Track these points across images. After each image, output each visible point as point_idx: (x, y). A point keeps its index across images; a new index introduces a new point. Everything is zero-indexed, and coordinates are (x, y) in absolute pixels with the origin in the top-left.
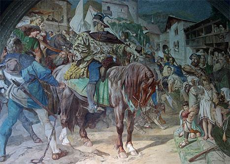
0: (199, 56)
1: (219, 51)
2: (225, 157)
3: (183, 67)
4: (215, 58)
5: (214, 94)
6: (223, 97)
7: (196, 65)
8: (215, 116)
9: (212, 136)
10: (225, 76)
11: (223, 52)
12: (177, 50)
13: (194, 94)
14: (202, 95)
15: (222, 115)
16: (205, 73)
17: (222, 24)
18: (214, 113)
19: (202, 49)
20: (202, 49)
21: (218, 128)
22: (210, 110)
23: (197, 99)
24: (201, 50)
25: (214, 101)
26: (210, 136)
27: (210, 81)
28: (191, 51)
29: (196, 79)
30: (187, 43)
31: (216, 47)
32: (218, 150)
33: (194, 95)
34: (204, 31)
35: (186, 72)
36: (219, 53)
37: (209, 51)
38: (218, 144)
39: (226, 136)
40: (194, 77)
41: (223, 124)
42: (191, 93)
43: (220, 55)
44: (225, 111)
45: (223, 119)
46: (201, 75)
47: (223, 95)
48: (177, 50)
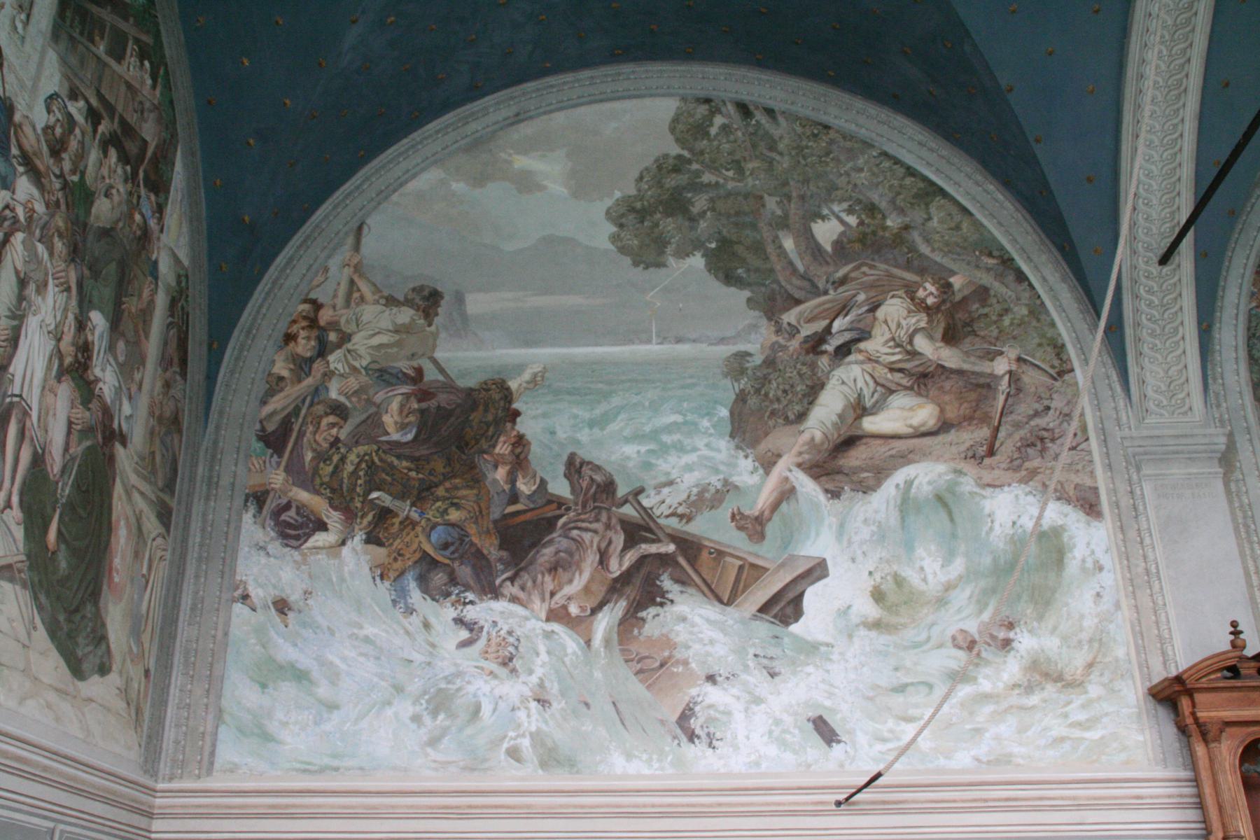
0: (71, 121)
1: (124, 158)
2: (35, 628)
3: (17, 117)
4: (105, 172)
5: (71, 317)
6: (85, 349)
7: (57, 150)
8: (51, 413)
9: (21, 502)
10: (113, 267)
11: (128, 168)
12: (20, 26)
13: (20, 266)
14: (38, 291)
15: (70, 424)
16: (67, 205)
17: (151, 63)
18: (50, 398)
19: (87, 102)
20: (87, 102)
21: (45, 476)
22: (45, 380)
23: (21, 298)
24: (81, 103)
25: (63, 345)
26: (15, 499)
27: (75, 253)
28: (57, 77)
29: (40, 208)
30: (56, 36)
31: (119, 132)
32: (24, 586)
33: (17, 272)
34: (106, 35)
35: (20, 147)
36: (119, 159)
37: (101, 128)
38: (29, 556)
39: (59, 532)
40: (36, 192)
41: (63, 470)
42: (9, 257)
43: (119, 171)
44: (80, 414)
45: (66, 449)
46: (57, 204)
47: (90, 338)
48: (20, 26)
